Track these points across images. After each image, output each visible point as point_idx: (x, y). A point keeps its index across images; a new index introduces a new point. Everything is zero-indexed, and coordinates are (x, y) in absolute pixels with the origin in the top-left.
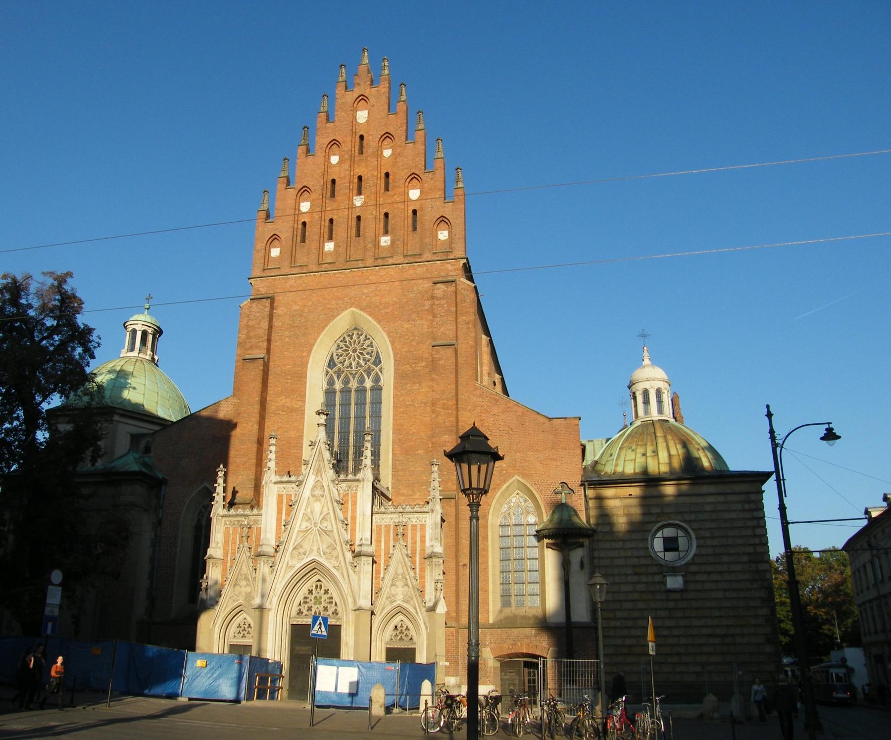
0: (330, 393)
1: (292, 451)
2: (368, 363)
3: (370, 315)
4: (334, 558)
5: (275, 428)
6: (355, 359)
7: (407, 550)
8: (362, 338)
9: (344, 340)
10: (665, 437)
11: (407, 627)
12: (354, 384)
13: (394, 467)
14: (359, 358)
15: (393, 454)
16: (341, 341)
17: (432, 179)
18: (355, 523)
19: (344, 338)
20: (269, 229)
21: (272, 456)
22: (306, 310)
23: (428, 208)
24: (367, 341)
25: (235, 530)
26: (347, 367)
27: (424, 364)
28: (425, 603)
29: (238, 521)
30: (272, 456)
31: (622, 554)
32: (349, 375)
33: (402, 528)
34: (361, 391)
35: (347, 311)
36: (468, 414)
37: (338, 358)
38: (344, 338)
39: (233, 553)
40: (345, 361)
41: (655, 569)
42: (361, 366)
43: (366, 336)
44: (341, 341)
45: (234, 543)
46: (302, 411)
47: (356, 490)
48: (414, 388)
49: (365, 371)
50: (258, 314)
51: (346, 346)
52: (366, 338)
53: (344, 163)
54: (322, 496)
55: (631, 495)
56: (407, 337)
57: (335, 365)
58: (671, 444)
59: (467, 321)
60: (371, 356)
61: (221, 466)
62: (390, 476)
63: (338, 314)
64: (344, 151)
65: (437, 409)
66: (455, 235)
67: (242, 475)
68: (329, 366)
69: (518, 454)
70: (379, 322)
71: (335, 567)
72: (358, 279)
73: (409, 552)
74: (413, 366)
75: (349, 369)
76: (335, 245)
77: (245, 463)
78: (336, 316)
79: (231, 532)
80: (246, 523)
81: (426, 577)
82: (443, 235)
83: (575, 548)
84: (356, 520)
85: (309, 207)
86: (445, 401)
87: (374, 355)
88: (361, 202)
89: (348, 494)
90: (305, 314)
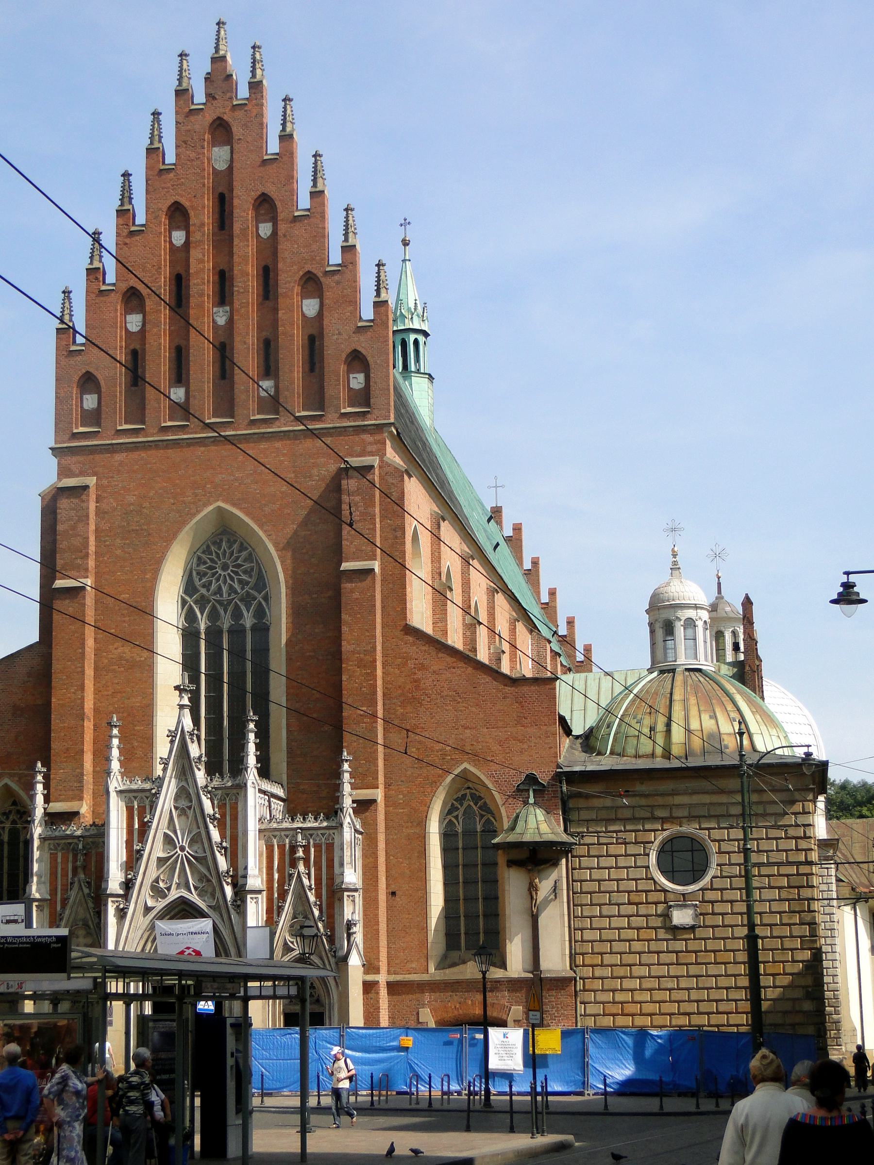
0: (189, 637)
1: (138, 728)
2: (247, 588)
3: (247, 514)
4: (209, 895)
5: (110, 693)
6: (225, 582)
7: (309, 879)
8: (235, 547)
9: (208, 551)
10: (685, 701)
11: (312, 984)
12: (226, 623)
13: (290, 752)
14: (232, 579)
15: (289, 732)
16: (204, 552)
17: (338, 283)
18: (237, 845)
19: (208, 547)
20: (79, 366)
21: (115, 753)
22: (147, 505)
23: (333, 335)
24: (244, 554)
25: (65, 860)
26: (215, 594)
27: (330, 593)
28: (335, 952)
29: (70, 844)
30: (115, 753)
31: (614, 874)
32: (218, 606)
33: (301, 850)
34: (237, 632)
35: (211, 508)
36: (397, 671)
37: (200, 580)
38: (208, 547)
39: (65, 890)
40: (210, 583)
41: (661, 897)
42: (236, 592)
43: (242, 544)
44: (204, 552)
45: (65, 874)
46: (150, 666)
47: (237, 799)
48: (317, 630)
49: (241, 600)
50: (73, 513)
51: (212, 560)
52: (242, 548)
53: (195, 248)
54: (190, 808)
55: (628, 791)
56: (304, 551)
57: (196, 590)
58: (694, 711)
59: (393, 527)
60: (251, 577)
61: (39, 765)
62: (285, 764)
63: (199, 512)
64: (194, 225)
65: (349, 668)
66: (375, 383)
67: (64, 769)
68: (186, 592)
69: (468, 731)
70: (261, 526)
71: (210, 906)
72: (225, 454)
73: (313, 882)
74: (315, 596)
75: (218, 597)
76: (187, 393)
77: (67, 749)
78: (194, 515)
79: (59, 860)
80: (80, 846)
81: (336, 916)
82: (357, 381)
83: (547, 868)
84: (237, 840)
85: (140, 324)
86: (362, 656)
87: (254, 573)
88: (224, 318)
89: (225, 804)
90: (145, 510)
